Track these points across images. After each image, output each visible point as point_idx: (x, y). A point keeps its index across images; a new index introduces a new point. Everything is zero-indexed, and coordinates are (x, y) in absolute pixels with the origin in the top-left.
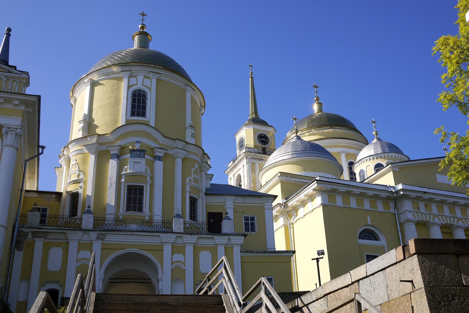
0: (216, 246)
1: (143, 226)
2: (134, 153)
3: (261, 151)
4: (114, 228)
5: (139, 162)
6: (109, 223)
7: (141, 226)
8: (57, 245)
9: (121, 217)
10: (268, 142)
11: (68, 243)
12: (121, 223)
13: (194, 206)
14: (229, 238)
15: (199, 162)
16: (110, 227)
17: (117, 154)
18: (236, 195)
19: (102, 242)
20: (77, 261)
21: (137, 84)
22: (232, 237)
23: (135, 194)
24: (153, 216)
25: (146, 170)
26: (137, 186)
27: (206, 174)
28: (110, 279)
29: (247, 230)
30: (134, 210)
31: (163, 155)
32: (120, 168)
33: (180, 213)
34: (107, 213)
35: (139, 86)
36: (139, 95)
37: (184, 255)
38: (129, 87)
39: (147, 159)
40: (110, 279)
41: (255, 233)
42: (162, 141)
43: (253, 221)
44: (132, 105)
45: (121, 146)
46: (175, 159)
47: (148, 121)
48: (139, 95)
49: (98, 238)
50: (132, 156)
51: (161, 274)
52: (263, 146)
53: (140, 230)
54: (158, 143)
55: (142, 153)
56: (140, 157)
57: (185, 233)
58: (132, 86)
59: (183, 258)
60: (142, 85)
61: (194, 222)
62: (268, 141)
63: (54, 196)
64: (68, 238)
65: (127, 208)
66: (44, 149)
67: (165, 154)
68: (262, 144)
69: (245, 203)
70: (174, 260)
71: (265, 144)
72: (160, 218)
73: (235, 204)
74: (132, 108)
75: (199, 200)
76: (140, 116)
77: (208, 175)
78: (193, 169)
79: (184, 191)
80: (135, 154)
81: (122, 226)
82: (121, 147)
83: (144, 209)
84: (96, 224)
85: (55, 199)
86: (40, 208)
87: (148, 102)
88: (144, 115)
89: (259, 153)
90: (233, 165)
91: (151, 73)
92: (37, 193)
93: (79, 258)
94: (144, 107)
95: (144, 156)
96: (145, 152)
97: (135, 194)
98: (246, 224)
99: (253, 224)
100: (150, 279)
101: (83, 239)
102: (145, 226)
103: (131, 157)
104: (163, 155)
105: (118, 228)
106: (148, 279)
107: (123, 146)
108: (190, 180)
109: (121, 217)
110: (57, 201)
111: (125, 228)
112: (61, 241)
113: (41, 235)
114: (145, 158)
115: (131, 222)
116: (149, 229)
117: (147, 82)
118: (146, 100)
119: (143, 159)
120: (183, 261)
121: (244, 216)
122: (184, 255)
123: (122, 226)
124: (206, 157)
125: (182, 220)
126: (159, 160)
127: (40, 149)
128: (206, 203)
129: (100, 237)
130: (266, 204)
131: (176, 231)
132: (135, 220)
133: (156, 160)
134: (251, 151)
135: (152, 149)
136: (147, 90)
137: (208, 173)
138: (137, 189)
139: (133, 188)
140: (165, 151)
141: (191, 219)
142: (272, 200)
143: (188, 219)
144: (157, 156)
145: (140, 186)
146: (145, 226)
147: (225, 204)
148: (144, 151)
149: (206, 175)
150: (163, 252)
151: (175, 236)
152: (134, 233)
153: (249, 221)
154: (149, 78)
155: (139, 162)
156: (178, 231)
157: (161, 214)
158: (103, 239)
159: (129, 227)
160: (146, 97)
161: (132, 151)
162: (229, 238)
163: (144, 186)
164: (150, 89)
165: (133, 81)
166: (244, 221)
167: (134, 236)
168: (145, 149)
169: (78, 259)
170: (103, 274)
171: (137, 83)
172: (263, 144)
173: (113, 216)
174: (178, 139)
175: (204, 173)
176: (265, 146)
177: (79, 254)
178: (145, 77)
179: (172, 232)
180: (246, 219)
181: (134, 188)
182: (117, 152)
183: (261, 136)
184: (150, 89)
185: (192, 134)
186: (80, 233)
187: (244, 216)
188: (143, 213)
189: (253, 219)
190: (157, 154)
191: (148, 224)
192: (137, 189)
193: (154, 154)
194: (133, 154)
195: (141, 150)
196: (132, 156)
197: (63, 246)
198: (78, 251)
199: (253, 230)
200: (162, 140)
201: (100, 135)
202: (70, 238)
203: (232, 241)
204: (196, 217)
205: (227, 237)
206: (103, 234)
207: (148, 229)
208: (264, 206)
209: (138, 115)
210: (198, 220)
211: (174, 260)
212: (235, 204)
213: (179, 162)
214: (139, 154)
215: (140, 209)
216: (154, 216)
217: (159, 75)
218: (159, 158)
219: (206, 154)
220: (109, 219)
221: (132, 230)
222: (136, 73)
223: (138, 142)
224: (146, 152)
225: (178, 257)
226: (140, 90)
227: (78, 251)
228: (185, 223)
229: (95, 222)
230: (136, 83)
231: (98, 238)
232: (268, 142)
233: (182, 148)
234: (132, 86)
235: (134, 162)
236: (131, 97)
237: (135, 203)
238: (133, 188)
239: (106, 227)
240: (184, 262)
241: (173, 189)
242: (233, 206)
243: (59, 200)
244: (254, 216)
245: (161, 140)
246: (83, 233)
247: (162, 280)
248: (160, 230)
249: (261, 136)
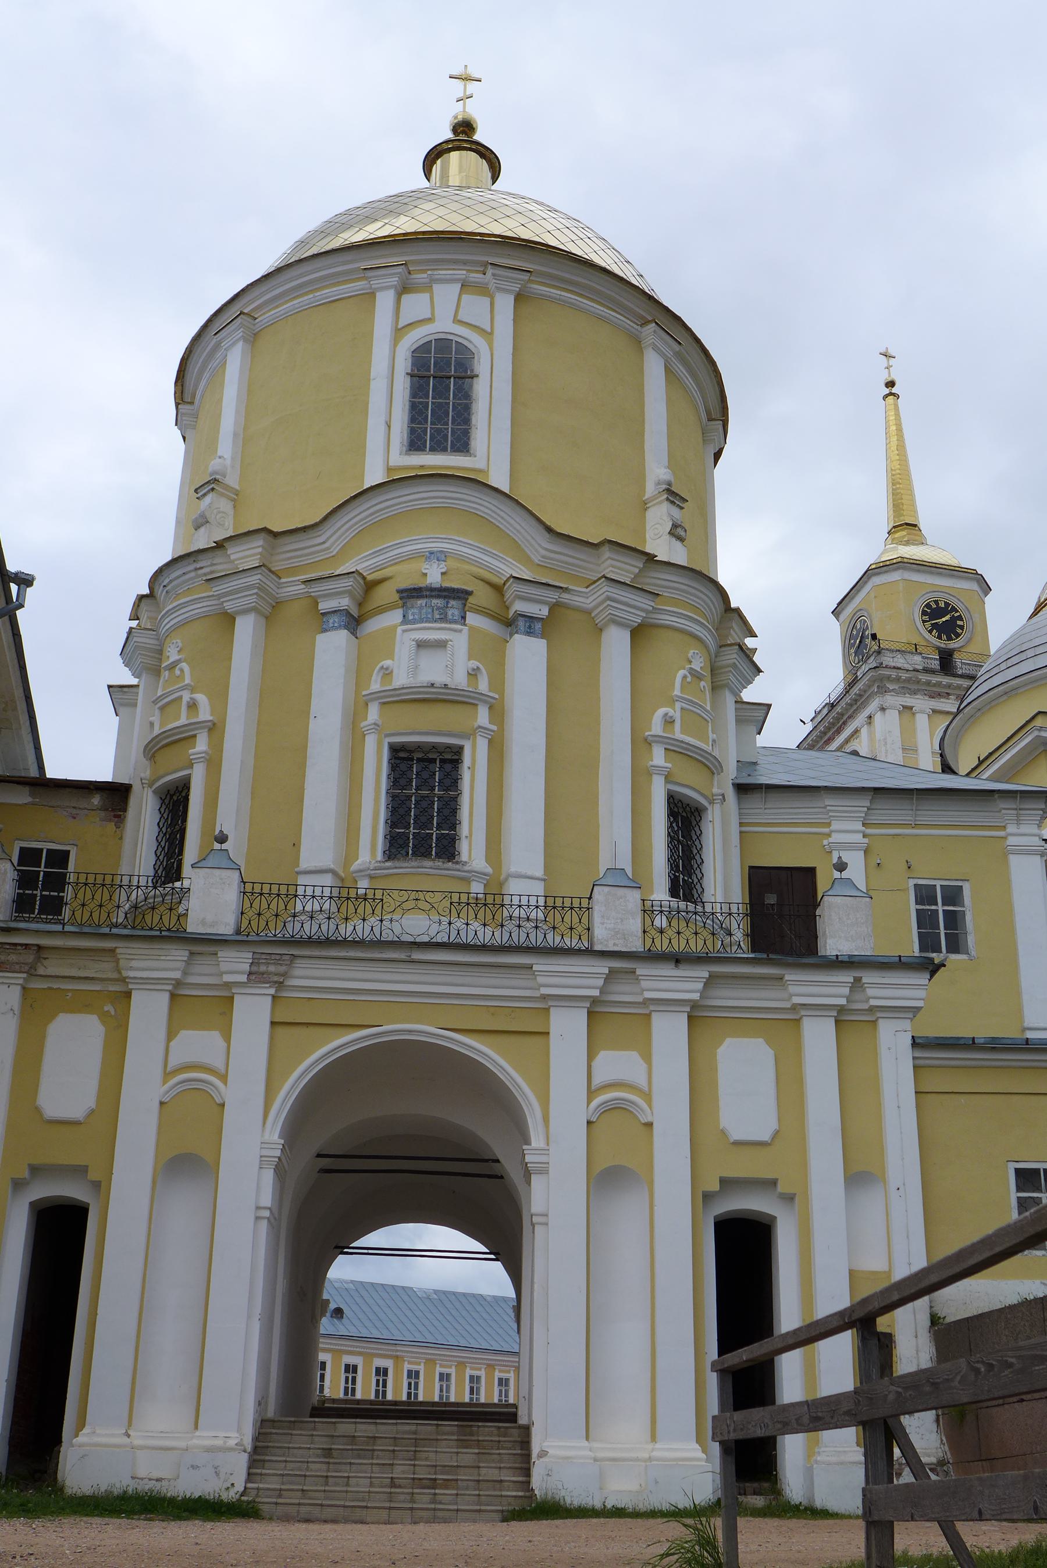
0: (797, 1017)
1: (458, 924)
2: (421, 602)
3: (936, 665)
4: (327, 929)
5: (441, 645)
6: (308, 908)
7: (450, 923)
8: (82, 1004)
9: (363, 884)
10: (959, 631)
11: (128, 995)
12: (360, 910)
13: (687, 835)
14: (858, 980)
15: (706, 647)
16: (309, 929)
17: (348, 613)
18: (878, 791)
19: (272, 991)
20: (167, 1075)
21: (429, 320)
22: (869, 977)
23: (425, 783)
24: (502, 877)
25: (473, 675)
26: (434, 747)
27: (739, 702)
28: (319, 1156)
29: (928, 942)
30: (422, 851)
31: (544, 611)
32: (359, 672)
33: (625, 863)
34: (304, 865)
35: (444, 325)
36: (443, 363)
38: (399, 332)
39: (473, 630)
40: (319, 1156)
41: (964, 957)
42: (543, 552)
43: (954, 905)
44: (413, 406)
45: (364, 578)
46: (601, 630)
47: (480, 471)
48: (443, 363)
49: (255, 976)
50: (411, 618)
51: (542, 1144)
52: (942, 644)
53: (445, 940)
54: (526, 560)
55: (452, 603)
56: (444, 619)
57: (652, 957)
60: (457, 321)
61: (691, 907)
62: (962, 627)
63: (96, 800)
64: (125, 973)
65: (391, 845)
66: (28, 589)
67: (555, 607)
68: (939, 637)
69: (916, 826)
70: (598, 1080)
71: (950, 639)
72: (538, 889)
73: (869, 831)
74: (412, 420)
75: (710, 812)
76: (444, 450)
77: (745, 706)
78: (681, 673)
79: (640, 776)
80: (421, 607)
81: (364, 920)
82: (362, 582)
83: (463, 847)
84: (251, 914)
85: (103, 814)
86: (41, 850)
87: (480, 389)
88: (462, 445)
89: (926, 670)
90: (830, 719)
91: (490, 271)
92: (27, 789)
93: (174, 1062)
94: (464, 415)
95: (464, 618)
96: (468, 599)
97: (425, 783)
98: (926, 920)
99: (954, 920)
100: (498, 1161)
101: (191, 979)
102: (467, 924)
103: (405, 620)
104: (544, 611)
105: (346, 931)
106: (487, 1161)
107: (369, 578)
108: (669, 721)
109: (363, 884)
110: (110, 820)
111: (377, 930)
112: (98, 988)
113: (13, 958)
114: (465, 625)
115: (405, 906)
116: (485, 935)
117: (475, 308)
118: (471, 386)
119: (459, 627)
120: (642, 1081)
121: (912, 883)
122: (647, 1056)
123: (364, 920)
124: (736, 625)
125: (635, 896)
126: (530, 632)
127: (14, 588)
128: (741, 824)
129: (263, 968)
130: (1011, 829)
131: (606, 945)
132: (421, 896)
133: (517, 632)
134: (899, 665)
135: (498, 589)
136: (477, 342)
137: (750, 694)
138: (436, 759)
139: (418, 759)
140: (552, 596)
141: (674, 892)
142: (1041, 812)
143: (660, 893)
144: (520, 618)
145: (449, 747)
146: (467, 924)
147: (826, 830)
148: (461, 595)
149: (739, 706)
151: (602, 967)
152: (417, 955)
153: (937, 904)
154: (482, 290)
155: (441, 645)
156: (614, 944)
157: (540, 872)
158: (276, 979)
159: (396, 927)
160: (472, 371)
161: (411, 594)
162: (858, 980)
163: (461, 748)
164: (488, 335)
165: (415, 305)
166: (913, 907)
167: (417, 966)
168: (465, 588)
169: (168, 1069)
170: (279, 1138)
171: (433, 314)
172: (944, 637)
173: (328, 880)
174: (610, 542)
175: (730, 701)
176: (952, 645)
177: (172, 1044)
178: (466, 286)
179: (589, 952)
180: (925, 895)
181: (420, 755)
182: (345, 602)
183: (934, 606)
184: (488, 335)
185: (675, 526)
186: (178, 954)
187: (915, 885)
188: (458, 866)
189: (953, 895)
190: (519, 606)
191: (481, 915)
192: (435, 760)
193: (508, 608)
194: (412, 607)
195: (446, 589)
196: (411, 618)
197: (106, 1009)
198: (171, 1035)
199: (955, 945)
200: (539, 546)
201: (276, 535)
202: (132, 974)
203: (870, 992)
204: (698, 887)
205: (847, 977)
206: (278, 957)
207: (480, 934)
208: (1005, 838)
209: (438, 447)
210: (707, 897)
211: (598, 1080)
212: (869, 831)
214: (438, 608)
215: (448, 850)
216: (506, 879)
217: (525, 277)
218: (531, 625)
219: (737, 611)
220: (309, 891)
221: (411, 939)
222: (429, 272)
223: (439, 556)
224: (471, 599)
226: (443, 344)
227: (171, 1035)
228: (648, 911)
229: (247, 904)
230: (430, 316)
231: (255, 976)
232: (959, 631)
233: (629, 583)
235: (421, 645)
236: (407, 374)
237: (424, 823)
238: (416, 755)
239: (293, 929)
240: (646, 1089)
241: (590, 765)
242: (864, 836)
243: (119, 816)
244: (959, 883)
245: (536, 546)
246: (192, 953)
247: (544, 1171)
248: (536, 939)
249: (934, 606)
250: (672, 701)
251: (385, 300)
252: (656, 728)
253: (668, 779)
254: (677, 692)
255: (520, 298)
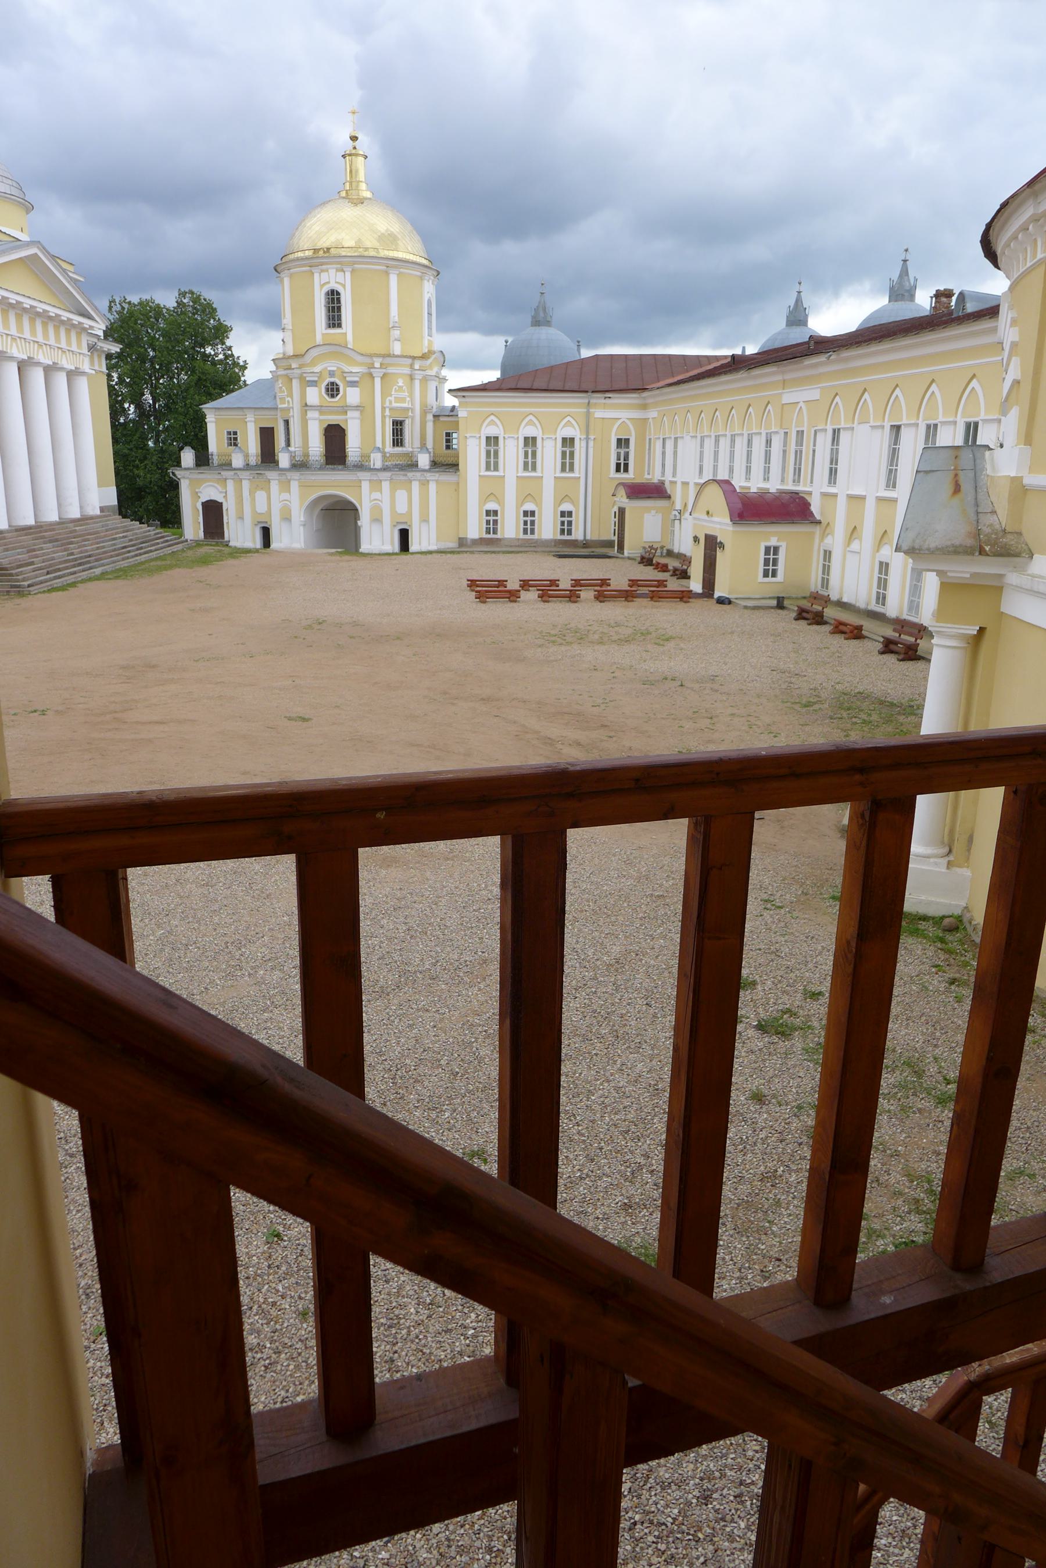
35: (333, 285)
37: (381, 493)
38: (322, 286)
58: (325, 284)
59: (380, 495)
60: (337, 282)
108: (390, 402)
143: (389, 448)
150: (361, 489)
184: (344, 286)
209: (334, 326)
213: (378, 381)
225: (376, 495)
227: (280, 494)
234: (325, 284)
250: (391, 395)
251: (316, 276)
252: (387, 404)
253: (390, 417)
254: (393, 393)
255: (353, 271)
